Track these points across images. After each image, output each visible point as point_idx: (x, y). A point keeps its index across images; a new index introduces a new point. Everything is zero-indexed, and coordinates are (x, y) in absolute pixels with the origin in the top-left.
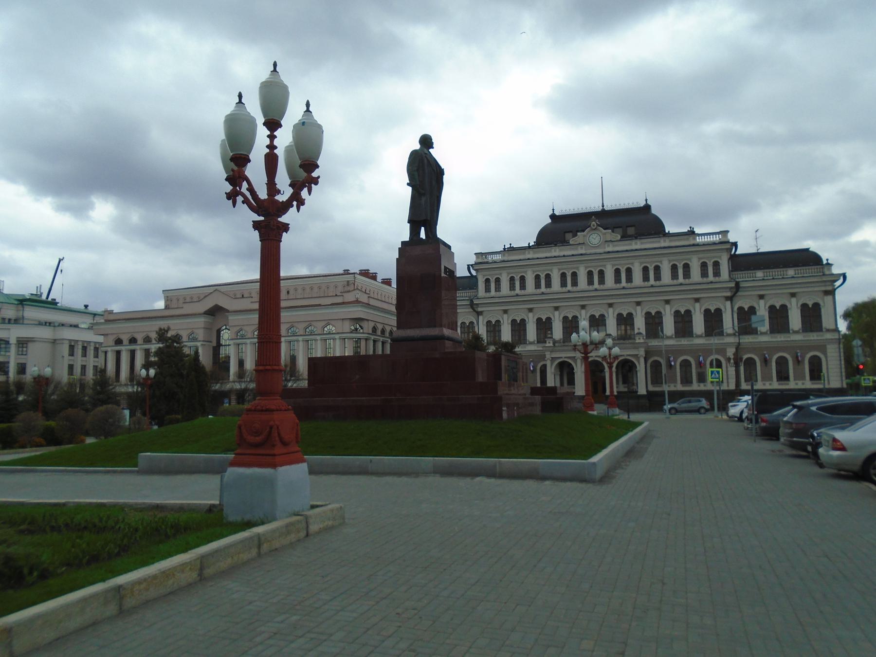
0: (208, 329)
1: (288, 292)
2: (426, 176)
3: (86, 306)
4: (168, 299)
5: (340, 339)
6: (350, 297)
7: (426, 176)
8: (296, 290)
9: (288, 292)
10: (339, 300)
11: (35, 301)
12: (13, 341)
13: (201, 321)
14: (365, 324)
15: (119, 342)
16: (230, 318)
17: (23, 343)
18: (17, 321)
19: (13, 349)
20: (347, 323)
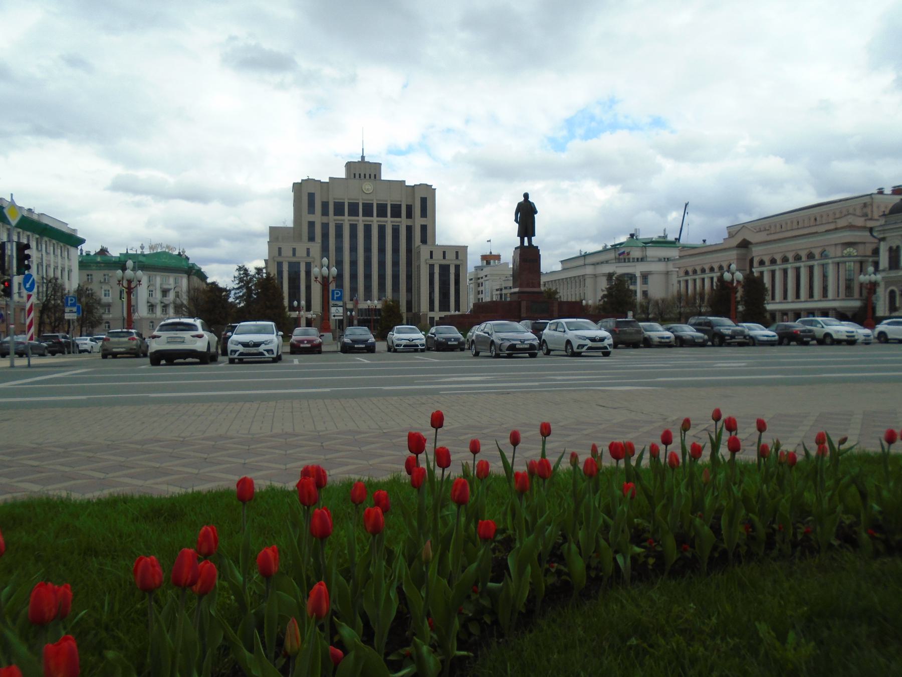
0: (740, 259)
1: (816, 219)
2: (526, 214)
3: (704, 241)
4: (729, 233)
5: (833, 263)
6: (842, 223)
7: (526, 214)
8: (822, 216)
9: (816, 219)
10: (832, 226)
11: (663, 242)
12: (638, 275)
13: (734, 254)
14: (861, 247)
15: (687, 273)
16: (754, 249)
17: (645, 277)
18: (642, 260)
19: (639, 281)
20: (839, 248)
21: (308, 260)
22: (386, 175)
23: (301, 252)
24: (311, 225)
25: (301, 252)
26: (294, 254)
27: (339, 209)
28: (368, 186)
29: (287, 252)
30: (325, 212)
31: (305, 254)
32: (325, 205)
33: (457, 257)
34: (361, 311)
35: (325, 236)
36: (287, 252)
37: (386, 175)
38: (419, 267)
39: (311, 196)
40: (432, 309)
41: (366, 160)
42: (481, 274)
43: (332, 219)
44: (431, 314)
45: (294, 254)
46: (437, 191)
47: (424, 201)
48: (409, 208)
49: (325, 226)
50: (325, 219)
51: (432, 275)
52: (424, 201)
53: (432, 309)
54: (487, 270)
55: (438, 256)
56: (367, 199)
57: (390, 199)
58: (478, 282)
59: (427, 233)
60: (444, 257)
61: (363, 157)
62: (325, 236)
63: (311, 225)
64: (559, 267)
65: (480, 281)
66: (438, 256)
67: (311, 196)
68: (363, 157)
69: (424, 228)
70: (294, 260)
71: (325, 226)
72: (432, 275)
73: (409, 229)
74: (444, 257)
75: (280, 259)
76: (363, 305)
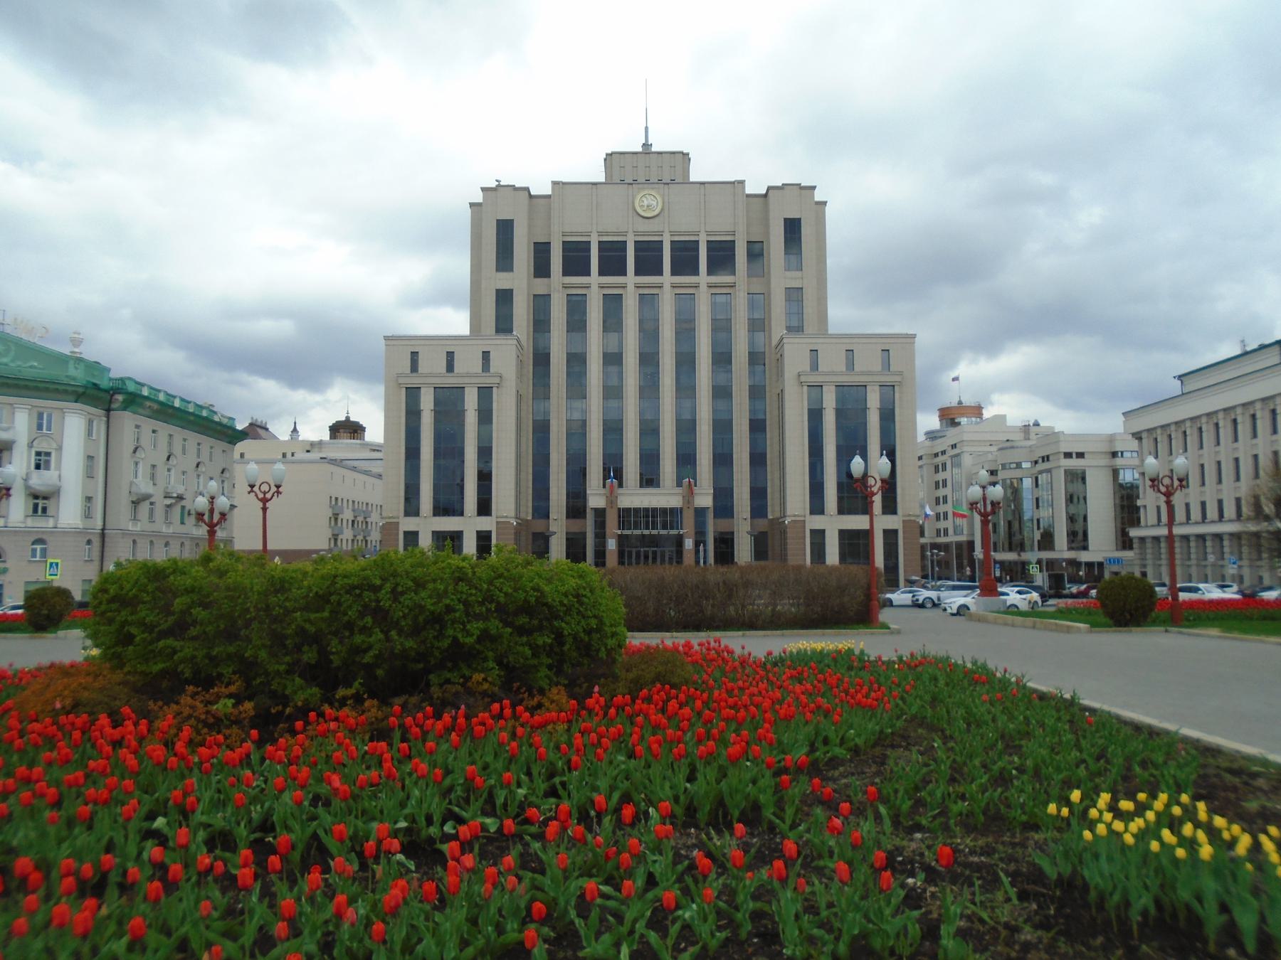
21: (486, 381)
22: (697, 173)
23: (468, 364)
24: (504, 297)
25: (468, 364)
26: (450, 367)
27: (576, 260)
28: (649, 201)
29: (433, 364)
30: (541, 268)
31: (477, 367)
32: (541, 252)
33: (887, 364)
34: (627, 516)
35: (541, 323)
36: (433, 364)
37: (697, 173)
38: (781, 396)
39: (505, 229)
40: (817, 506)
41: (654, 149)
42: (940, 445)
43: (558, 284)
44: (816, 522)
45: (450, 367)
46: (829, 210)
47: (793, 228)
48: (756, 252)
49: (541, 305)
50: (540, 286)
51: (815, 416)
52: (793, 228)
53: (817, 506)
54: (952, 435)
55: (832, 362)
56: (647, 231)
57: (703, 227)
58: (939, 462)
59: (802, 308)
60: (850, 364)
61: (646, 145)
62: (541, 323)
63: (504, 297)
64: (1176, 387)
65: (941, 459)
66: (832, 362)
67: (505, 229)
68: (646, 145)
69: (794, 295)
70: (451, 381)
71: (541, 305)
72: (815, 416)
73: (759, 301)
74: (850, 364)
75: (414, 381)
76: (634, 497)
